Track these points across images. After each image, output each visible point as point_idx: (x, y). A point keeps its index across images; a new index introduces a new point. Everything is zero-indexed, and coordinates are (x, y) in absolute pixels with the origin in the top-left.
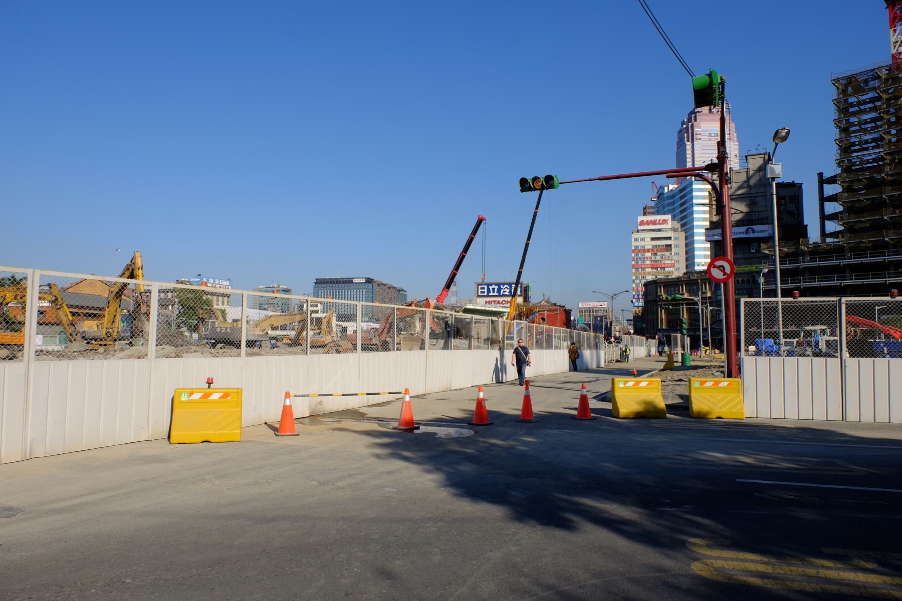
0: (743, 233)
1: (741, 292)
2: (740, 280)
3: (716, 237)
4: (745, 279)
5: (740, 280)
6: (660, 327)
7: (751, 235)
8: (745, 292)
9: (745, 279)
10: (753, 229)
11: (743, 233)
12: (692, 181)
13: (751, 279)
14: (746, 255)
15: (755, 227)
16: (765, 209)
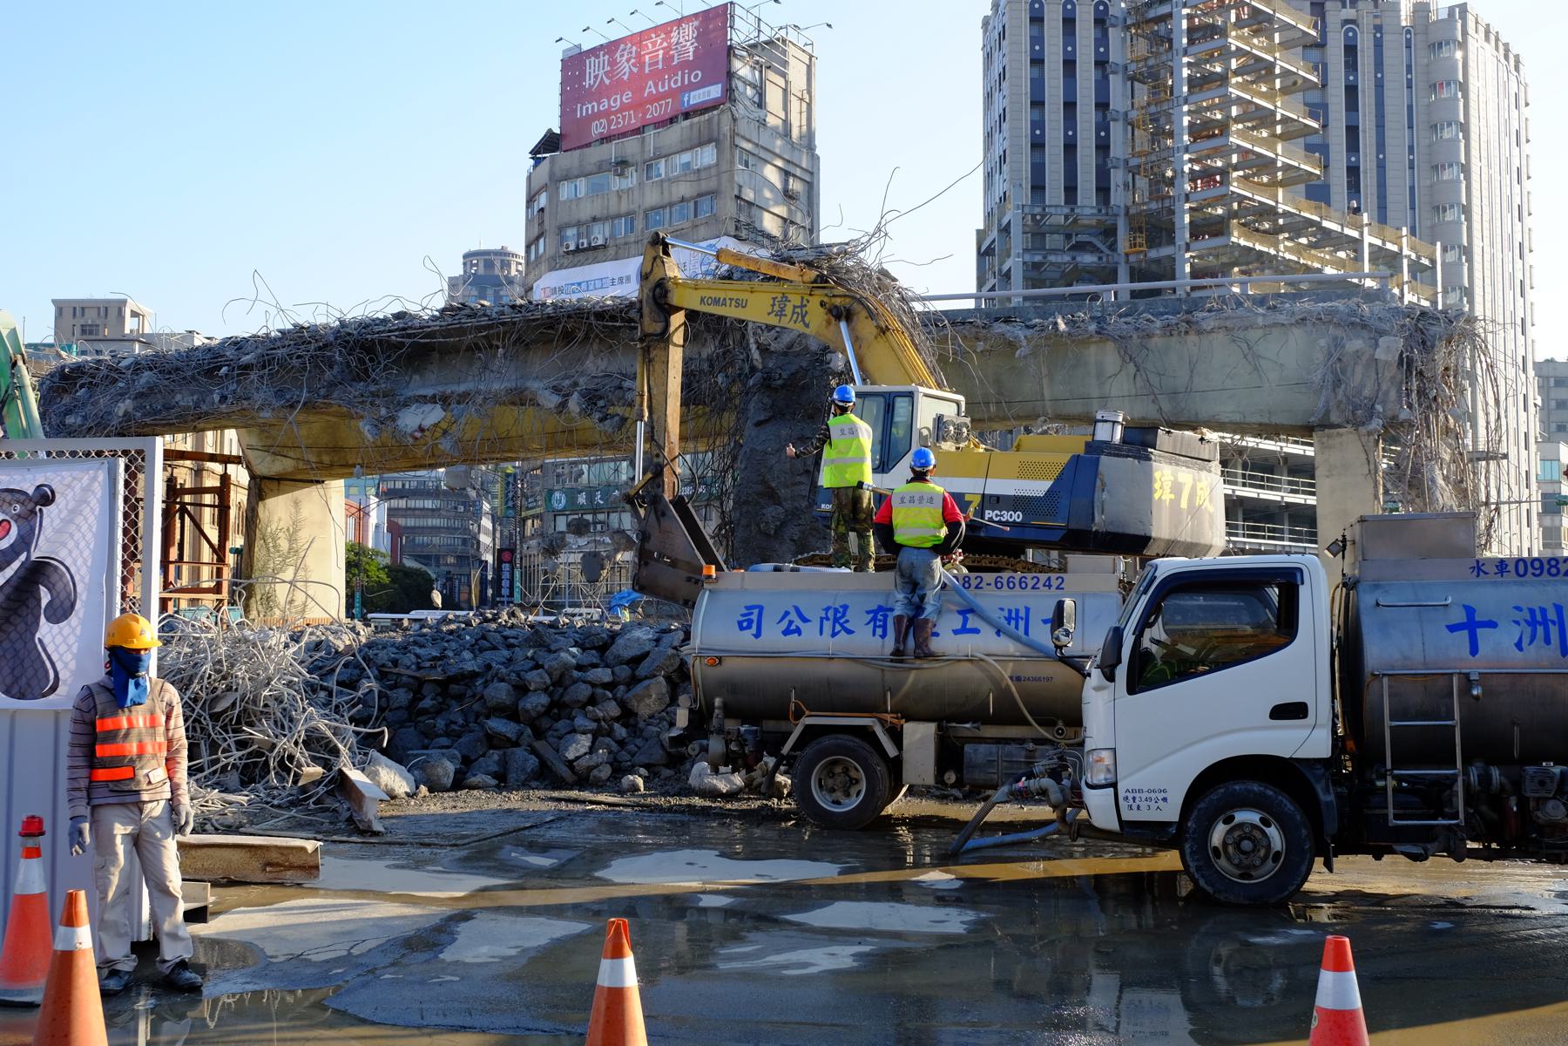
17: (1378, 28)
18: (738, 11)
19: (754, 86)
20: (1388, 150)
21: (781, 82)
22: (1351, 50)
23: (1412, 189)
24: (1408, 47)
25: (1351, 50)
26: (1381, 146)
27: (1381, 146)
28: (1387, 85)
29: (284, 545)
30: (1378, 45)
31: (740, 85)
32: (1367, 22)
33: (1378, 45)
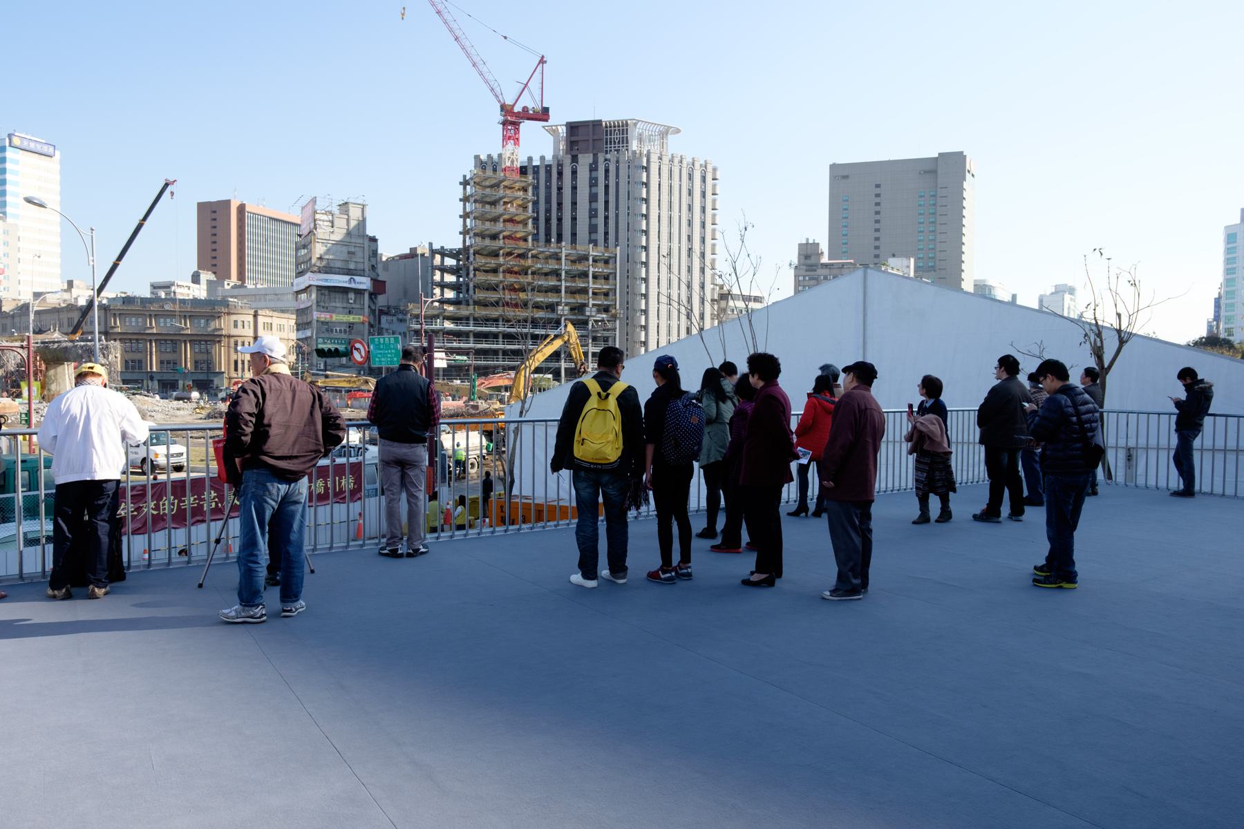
0: (346, 282)
1: (340, 341)
2: (338, 329)
3: (321, 282)
4: (343, 329)
5: (338, 329)
6: (149, 370)
7: (353, 286)
8: (343, 342)
9: (343, 329)
10: (354, 280)
11: (346, 282)
12: (5, 147)
13: (348, 329)
14: (345, 305)
15: (357, 278)
16: (362, 261)
17: (617, 162)
18: (318, 199)
19: (330, 221)
20: (620, 209)
21: (346, 217)
22: (607, 171)
23: (628, 224)
24: (629, 168)
25: (607, 171)
26: (617, 208)
27: (617, 208)
28: (620, 184)
29: (53, 378)
30: (617, 168)
31: (321, 223)
32: (613, 160)
33: (617, 168)
